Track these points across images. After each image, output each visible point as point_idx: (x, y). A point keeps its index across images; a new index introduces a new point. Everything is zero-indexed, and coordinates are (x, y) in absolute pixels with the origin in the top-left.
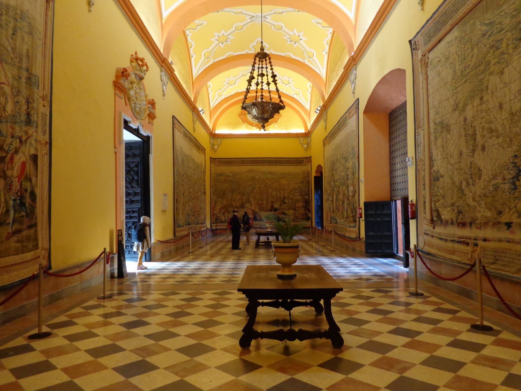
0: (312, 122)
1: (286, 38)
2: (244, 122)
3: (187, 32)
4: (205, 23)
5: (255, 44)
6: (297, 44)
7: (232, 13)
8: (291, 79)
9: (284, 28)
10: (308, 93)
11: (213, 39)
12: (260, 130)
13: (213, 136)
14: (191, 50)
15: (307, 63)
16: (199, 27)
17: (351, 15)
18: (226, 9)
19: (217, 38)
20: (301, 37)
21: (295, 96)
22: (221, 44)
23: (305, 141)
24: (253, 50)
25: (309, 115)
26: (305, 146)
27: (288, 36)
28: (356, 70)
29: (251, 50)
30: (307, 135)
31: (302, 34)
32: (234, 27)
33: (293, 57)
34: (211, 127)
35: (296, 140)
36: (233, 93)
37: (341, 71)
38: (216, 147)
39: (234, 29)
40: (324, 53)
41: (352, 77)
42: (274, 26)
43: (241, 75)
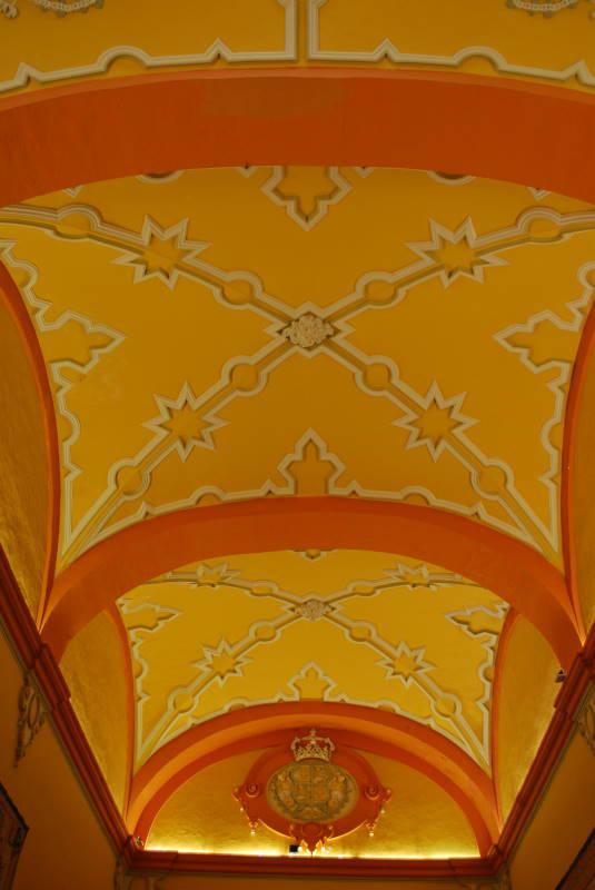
0: (507, 808)
1: (402, 423)
2: (253, 820)
3: (55, 371)
5: (298, 456)
6: (443, 444)
7: (217, 291)
10: (480, 704)
11: (151, 425)
12: (312, 848)
14: (66, 448)
15: (486, 518)
19: (165, 417)
20: (456, 415)
22: (178, 444)
24: (291, 482)
25: (491, 786)
27: (412, 416)
31: (458, 401)
33: (436, 502)
34: (130, 826)
36: (226, 709)
40: (545, 480)
43: (252, 636)
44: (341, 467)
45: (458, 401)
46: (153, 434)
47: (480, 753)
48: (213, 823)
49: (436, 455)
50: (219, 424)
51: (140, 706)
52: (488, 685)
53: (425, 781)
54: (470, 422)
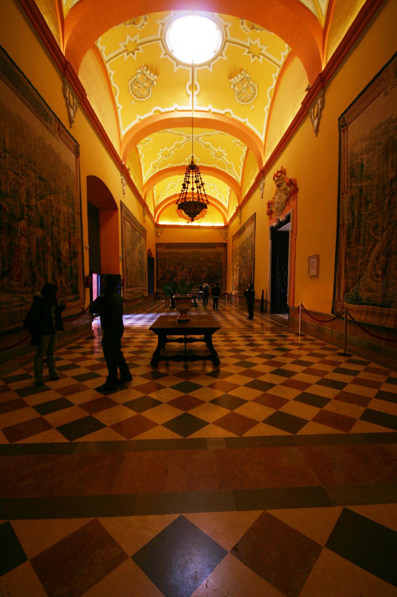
2: (180, 217)
4: (152, 140)
6: (220, 158)
8: (215, 186)
9: (211, 147)
13: (157, 226)
15: (228, 173)
16: (147, 143)
17: (262, 138)
18: (169, 130)
19: (162, 153)
21: (217, 198)
23: (224, 232)
26: (224, 235)
27: (214, 153)
28: (264, 179)
29: (186, 162)
30: (226, 227)
32: (175, 144)
35: (218, 231)
37: (253, 181)
38: (159, 234)
39: (174, 146)
41: (261, 185)
42: (204, 145)
44: (199, 160)
45: (224, 151)
46: (159, 156)
47: (226, 206)
48: (171, 217)
49: (219, 160)
50: (173, 153)
51: (155, 195)
52: (229, 192)
53: (215, 209)
54: (226, 155)
